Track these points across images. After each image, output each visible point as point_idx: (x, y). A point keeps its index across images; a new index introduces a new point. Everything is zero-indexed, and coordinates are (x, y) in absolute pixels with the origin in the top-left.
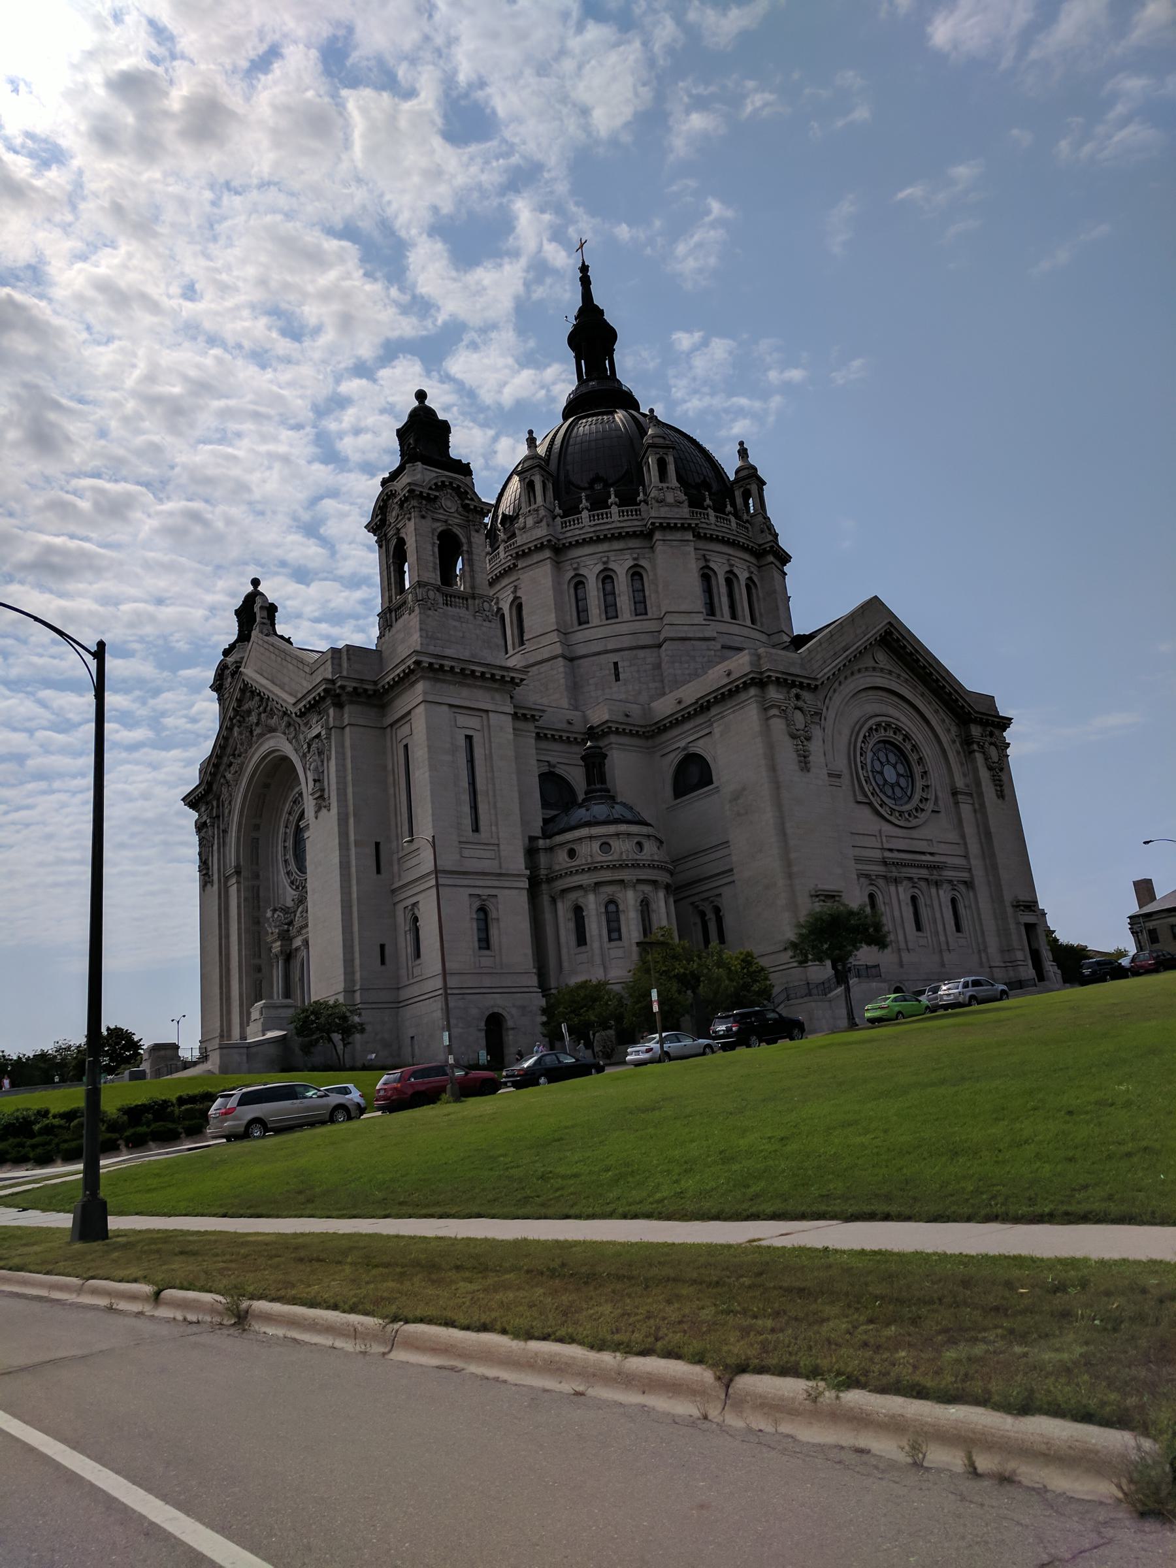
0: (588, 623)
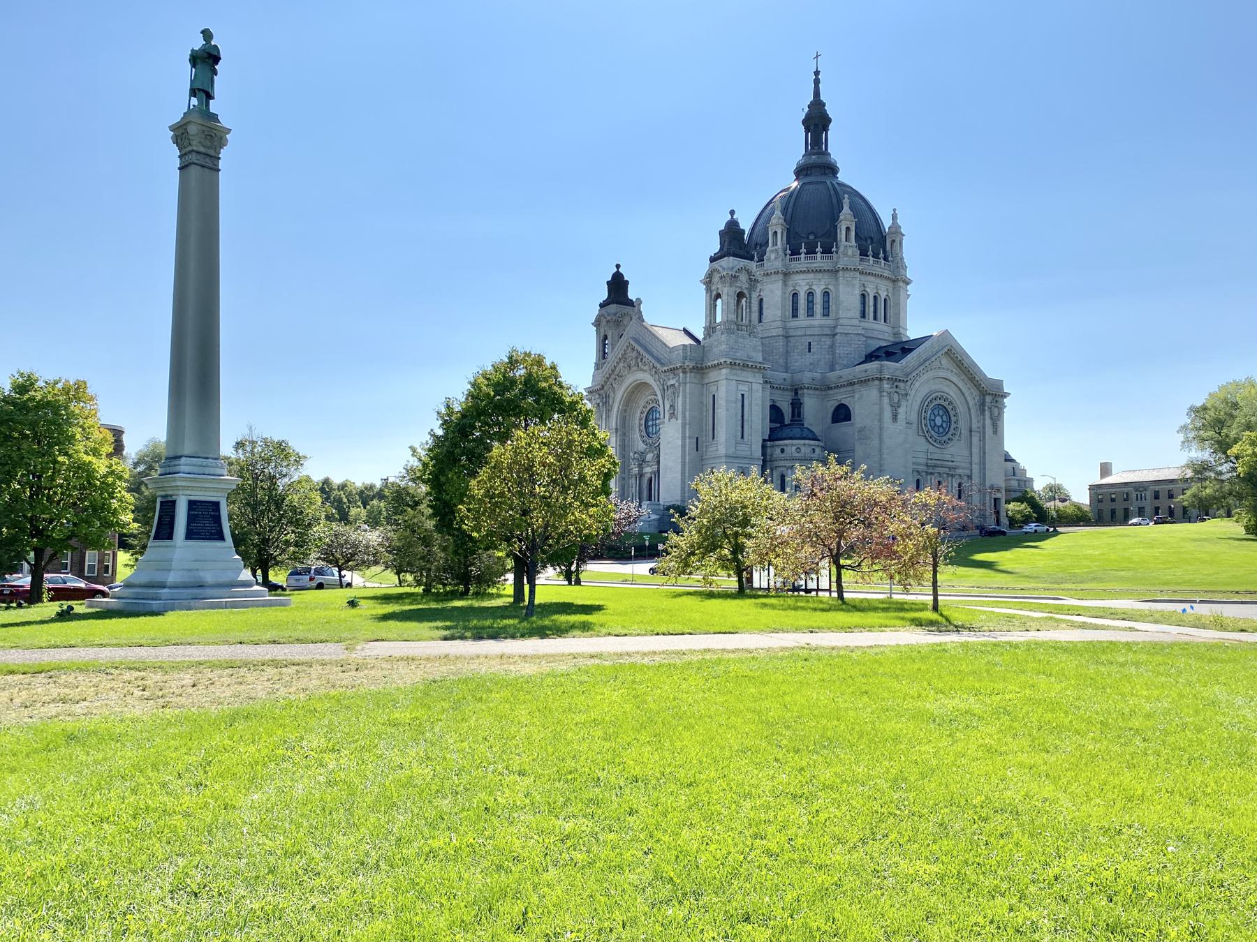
0: (797, 316)
